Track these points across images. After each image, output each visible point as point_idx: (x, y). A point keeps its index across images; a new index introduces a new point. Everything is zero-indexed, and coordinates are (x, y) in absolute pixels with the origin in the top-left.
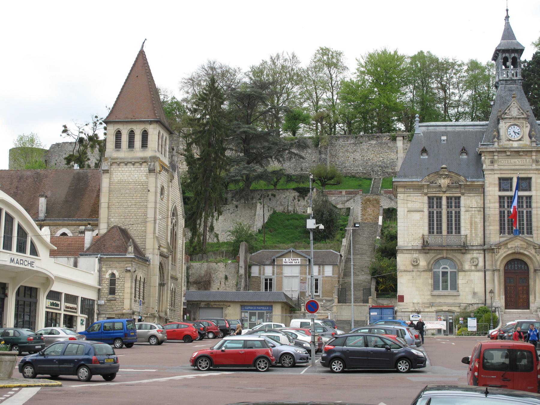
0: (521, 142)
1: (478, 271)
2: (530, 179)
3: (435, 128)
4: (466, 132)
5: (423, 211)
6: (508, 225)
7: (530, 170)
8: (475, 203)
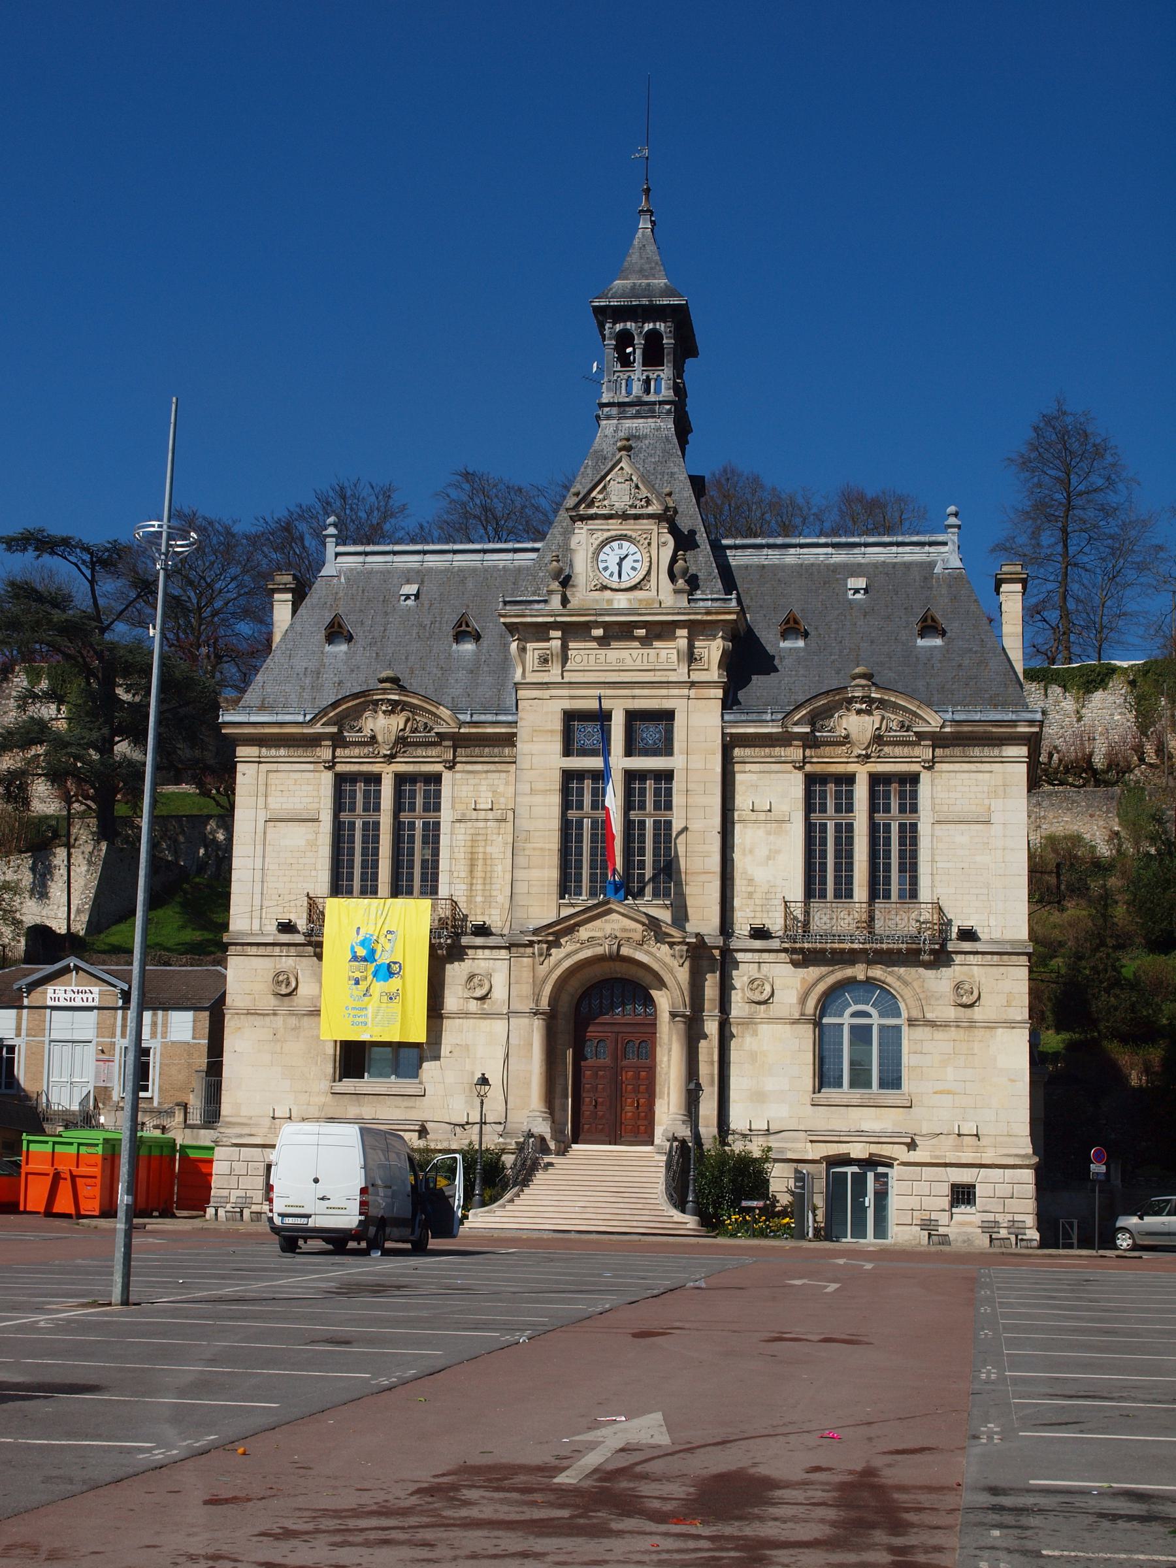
1: (486, 1016)
2: (668, 716)
3: (389, 558)
4: (486, 570)
5: (317, 820)
6: (593, 866)
7: (668, 684)
8: (490, 794)
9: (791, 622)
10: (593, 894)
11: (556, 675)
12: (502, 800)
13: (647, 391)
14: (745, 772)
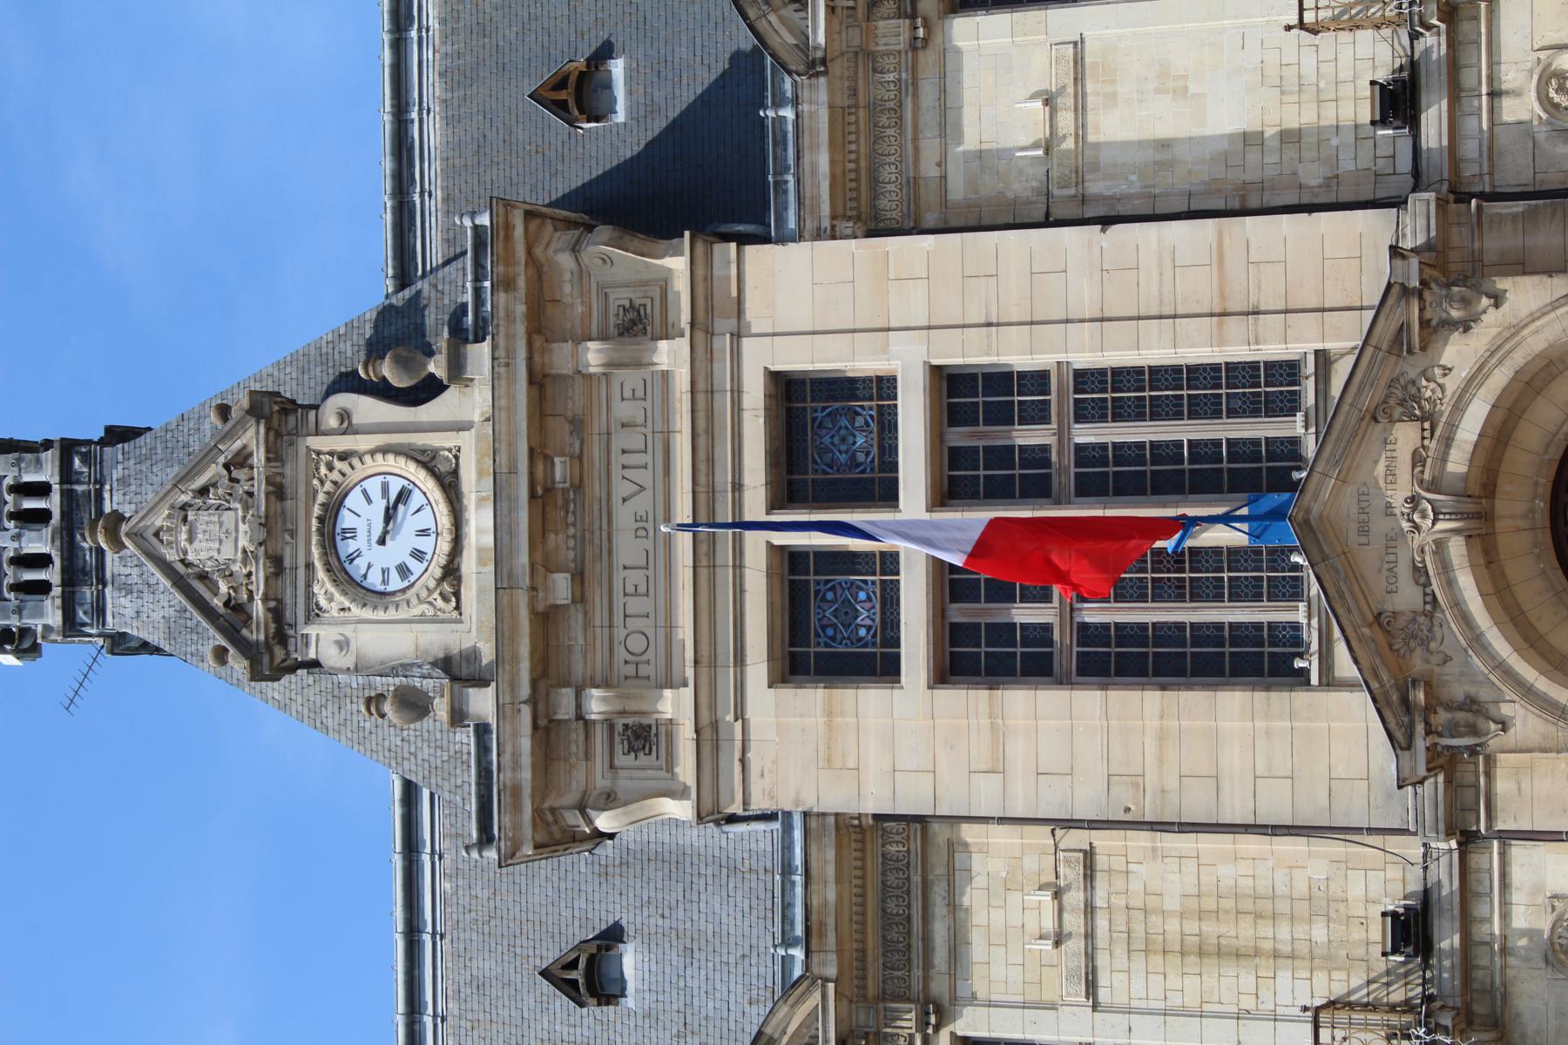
0: (473, 484)
7: (703, 390)
8: (1015, 898)
9: (562, 95)
10: (1291, 590)
11: (676, 704)
12: (1030, 863)
13: (42, 517)
14: (944, 178)
